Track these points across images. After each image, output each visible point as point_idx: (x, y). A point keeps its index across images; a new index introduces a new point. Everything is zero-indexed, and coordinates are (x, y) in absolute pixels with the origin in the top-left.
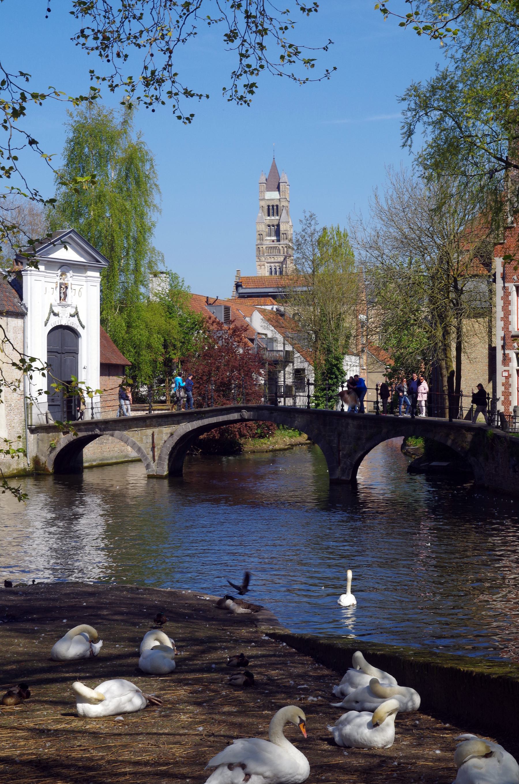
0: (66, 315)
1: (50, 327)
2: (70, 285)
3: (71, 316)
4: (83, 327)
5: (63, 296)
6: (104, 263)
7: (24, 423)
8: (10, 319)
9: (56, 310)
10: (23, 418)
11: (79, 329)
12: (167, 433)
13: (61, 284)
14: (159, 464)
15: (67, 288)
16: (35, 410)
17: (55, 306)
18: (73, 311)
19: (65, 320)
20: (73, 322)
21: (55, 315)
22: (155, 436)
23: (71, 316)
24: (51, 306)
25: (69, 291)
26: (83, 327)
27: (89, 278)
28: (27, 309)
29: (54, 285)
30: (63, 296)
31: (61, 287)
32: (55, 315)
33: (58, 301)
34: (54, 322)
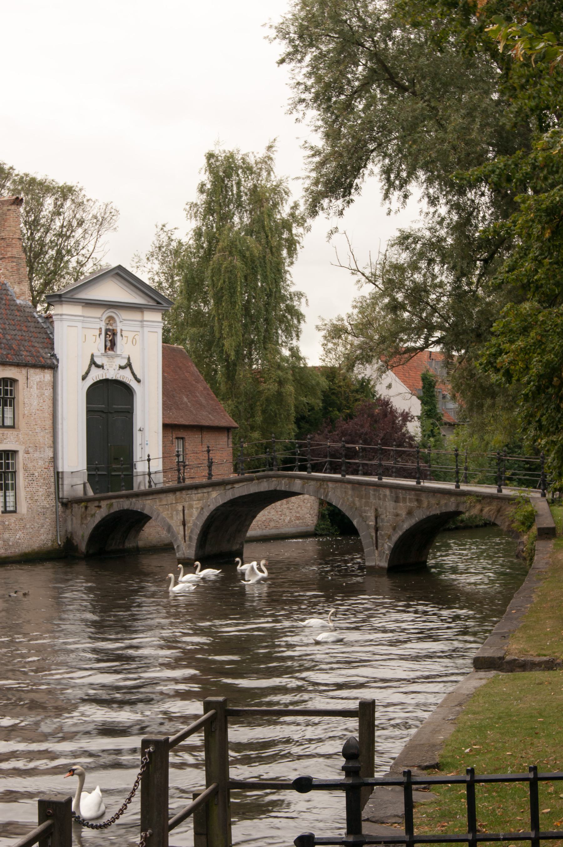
0: (114, 366)
1: (90, 381)
2: (119, 331)
3: (121, 367)
4: (139, 381)
6: (165, 305)
7: (53, 496)
8: (32, 371)
9: (98, 361)
10: (52, 489)
11: (133, 384)
12: (197, 508)
13: (107, 330)
14: (189, 546)
15: (114, 334)
16: (67, 481)
17: (98, 356)
18: (124, 362)
20: (126, 376)
22: (186, 511)
23: (121, 367)
24: (92, 356)
25: (118, 339)
26: (139, 381)
27: (145, 323)
28: (58, 360)
29: (98, 332)
30: (111, 345)
31: (106, 334)
33: (103, 351)
34: (96, 375)
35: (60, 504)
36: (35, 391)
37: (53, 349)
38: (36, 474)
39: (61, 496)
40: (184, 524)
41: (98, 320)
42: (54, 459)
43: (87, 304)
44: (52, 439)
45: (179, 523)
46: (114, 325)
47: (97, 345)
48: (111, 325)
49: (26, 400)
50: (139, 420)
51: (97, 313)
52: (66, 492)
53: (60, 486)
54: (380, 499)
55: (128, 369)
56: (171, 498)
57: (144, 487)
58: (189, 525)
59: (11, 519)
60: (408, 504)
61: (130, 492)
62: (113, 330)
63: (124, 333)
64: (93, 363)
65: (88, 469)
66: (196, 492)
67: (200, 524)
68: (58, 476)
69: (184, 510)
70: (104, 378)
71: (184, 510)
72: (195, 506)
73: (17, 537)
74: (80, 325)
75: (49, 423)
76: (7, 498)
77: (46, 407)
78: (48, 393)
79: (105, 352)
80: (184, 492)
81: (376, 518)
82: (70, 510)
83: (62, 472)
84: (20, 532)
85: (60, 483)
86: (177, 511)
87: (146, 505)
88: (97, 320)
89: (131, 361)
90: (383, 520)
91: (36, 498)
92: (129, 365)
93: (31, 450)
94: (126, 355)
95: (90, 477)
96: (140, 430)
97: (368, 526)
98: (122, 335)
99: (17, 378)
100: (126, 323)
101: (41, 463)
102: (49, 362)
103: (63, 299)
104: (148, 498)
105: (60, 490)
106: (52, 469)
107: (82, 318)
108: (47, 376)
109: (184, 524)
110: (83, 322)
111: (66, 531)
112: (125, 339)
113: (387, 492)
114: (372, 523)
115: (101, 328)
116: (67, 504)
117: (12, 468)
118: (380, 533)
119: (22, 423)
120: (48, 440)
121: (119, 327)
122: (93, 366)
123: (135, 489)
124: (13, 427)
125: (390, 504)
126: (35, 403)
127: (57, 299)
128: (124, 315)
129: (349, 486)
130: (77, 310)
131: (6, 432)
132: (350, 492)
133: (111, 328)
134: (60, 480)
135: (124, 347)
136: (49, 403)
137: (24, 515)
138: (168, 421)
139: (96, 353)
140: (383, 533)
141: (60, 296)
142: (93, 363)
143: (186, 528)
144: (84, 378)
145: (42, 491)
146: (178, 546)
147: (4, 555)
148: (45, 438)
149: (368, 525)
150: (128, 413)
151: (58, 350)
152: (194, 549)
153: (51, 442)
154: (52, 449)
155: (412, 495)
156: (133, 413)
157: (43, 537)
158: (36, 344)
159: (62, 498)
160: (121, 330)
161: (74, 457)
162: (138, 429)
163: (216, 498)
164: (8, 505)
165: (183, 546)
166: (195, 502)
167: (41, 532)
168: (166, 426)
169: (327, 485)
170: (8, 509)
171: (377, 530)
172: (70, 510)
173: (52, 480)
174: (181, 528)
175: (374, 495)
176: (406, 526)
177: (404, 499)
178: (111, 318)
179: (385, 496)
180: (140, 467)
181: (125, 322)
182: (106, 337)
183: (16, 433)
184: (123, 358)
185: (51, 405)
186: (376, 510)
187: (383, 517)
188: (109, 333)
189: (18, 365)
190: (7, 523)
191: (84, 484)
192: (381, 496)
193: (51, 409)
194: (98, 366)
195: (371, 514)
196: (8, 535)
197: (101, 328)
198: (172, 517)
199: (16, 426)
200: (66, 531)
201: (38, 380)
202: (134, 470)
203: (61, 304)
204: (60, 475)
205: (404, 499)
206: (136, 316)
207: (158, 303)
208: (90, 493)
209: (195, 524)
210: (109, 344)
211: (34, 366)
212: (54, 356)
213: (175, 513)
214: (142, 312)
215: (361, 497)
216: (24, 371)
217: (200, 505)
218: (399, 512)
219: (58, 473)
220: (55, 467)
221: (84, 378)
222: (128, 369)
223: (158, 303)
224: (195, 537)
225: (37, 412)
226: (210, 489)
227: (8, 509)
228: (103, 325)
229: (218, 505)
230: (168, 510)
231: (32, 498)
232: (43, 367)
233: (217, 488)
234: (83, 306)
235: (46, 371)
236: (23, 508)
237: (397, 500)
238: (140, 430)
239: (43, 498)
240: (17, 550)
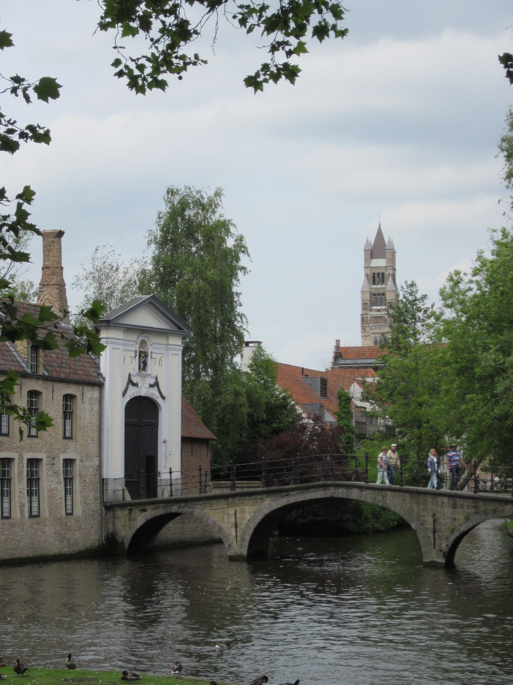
0: (146, 385)
1: (128, 398)
2: (149, 353)
3: (151, 386)
4: (163, 398)
5: (143, 366)
6: (186, 331)
7: (99, 500)
8: (86, 388)
9: (135, 380)
10: (98, 495)
11: (160, 400)
12: (250, 512)
13: (140, 352)
14: (241, 546)
15: (146, 356)
16: (111, 487)
17: (134, 376)
18: (153, 381)
19: (144, 391)
20: (153, 393)
21: (135, 385)
22: (237, 515)
23: (151, 386)
24: (130, 375)
25: (149, 360)
26: (163, 398)
27: (170, 346)
28: (104, 379)
29: (133, 354)
30: (143, 366)
31: (140, 356)
32: (135, 385)
33: (137, 371)
34: (133, 392)
35: (103, 508)
36: (87, 406)
38: (88, 480)
39: (105, 500)
41: (134, 343)
42: (100, 467)
43: (128, 328)
44: (98, 449)
46: (146, 348)
47: (133, 366)
48: (144, 348)
49: (82, 414)
51: (134, 337)
52: (110, 497)
53: (105, 491)
54: (438, 506)
55: (156, 387)
57: (166, 495)
58: (242, 526)
59: (71, 521)
60: (466, 510)
61: (153, 499)
62: (145, 352)
63: (153, 355)
64: (130, 382)
65: (126, 475)
66: (249, 498)
67: (253, 526)
68: (103, 482)
69: (236, 514)
70: (138, 395)
71: (236, 514)
72: (247, 511)
73: (76, 537)
74: (121, 347)
75: (96, 434)
76: (33, 503)
77: (94, 420)
78: (96, 407)
79: (139, 372)
80: (237, 498)
81: (434, 521)
82: (112, 513)
83: (107, 479)
84: (78, 532)
85: (105, 488)
86: (228, 515)
89: (158, 380)
90: (440, 524)
91: (88, 502)
92: (156, 384)
93: (84, 459)
94: (154, 375)
95: (128, 484)
96: (164, 442)
97: (427, 529)
98: (151, 357)
99: (76, 394)
100: (155, 347)
101: (91, 470)
103: (111, 324)
104: (197, 503)
105: (105, 495)
106: (98, 476)
107: (123, 342)
108: (94, 393)
110: (124, 345)
111: (108, 532)
112: (154, 360)
113: (446, 500)
115: (136, 351)
116: (110, 507)
117: (36, 476)
118: (438, 536)
119: (78, 435)
121: (150, 349)
122: (130, 384)
123: (159, 497)
124: (71, 438)
125: (448, 511)
126: (87, 417)
127: (105, 324)
130: (118, 334)
131: (68, 443)
132: (408, 500)
133: (143, 350)
134: (105, 485)
135: (152, 367)
136: (96, 416)
137: (80, 517)
138: (186, 435)
139: (133, 373)
140: (440, 534)
141: (108, 322)
142: (130, 382)
143: (238, 530)
144: (124, 394)
146: (230, 545)
147: (68, 553)
148: (93, 448)
149: (426, 528)
150: (154, 426)
152: (246, 548)
153: (97, 452)
154: (98, 458)
155: (470, 503)
156: (157, 427)
157: (92, 537)
158: (85, 364)
159: (106, 502)
160: (151, 353)
161: (115, 467)
162: (163, 441)
164: (33, 510)
165: (235, 545)
166: (247, 507)
167: (91, 532)
168: (185, 440)
169: (386, 494)
170: (33, 514)
171: (434, 532)
172: (112, 513)
173: (99, 486)
174: (233, 530)
175: (433, 502)
177: (462, 506)
178: (143, 343)
179: (443, 503)
180: (164, 476)
181: (154, 345)
182: (139, 359)
183: (75, 443)
184: (152, 377)
185: (98, 419)
186: (434, 515)
187: (441, 520)
188: (143, 355)
190: (69, 524)
191: (123, 490)
192: (440, 503)
193: (98, 422)
195: (430, 520)
196: (69, 535)
197: (136, 351)
198: (223, 520)
199: (73, 437)
200: (108, 532)
201: (90, 396)
202: (159, 478)
203: (107, 329)
204: (105, 481)
205: (462, 506)
206: (162, 340)
207: (180, 328)
208: (128, 498)
209: (247, 527)
210: (142, 365)
212: (100, 374)
213: (226, 516)
214: (167, 337)
215: (419, 504)
216: (81, 388)
217: (253, 510)
218: (457, 517)
219: (103, 479)
220: (100, 474)
221: (124, 394)
222: (156, 387)
223: (180, 328)
225: (89, 425)
226: (264, 496)
227: (33, 514)
228: (137, 348)
229: (272, 509)
230: (219, 513)
231: (85, 502)
233: (271, 495)
234: (124, 331)
235: (95, 388)
237: (455, 507)
238: (164, 442)
239: (92, 502)
240: (76, 549)
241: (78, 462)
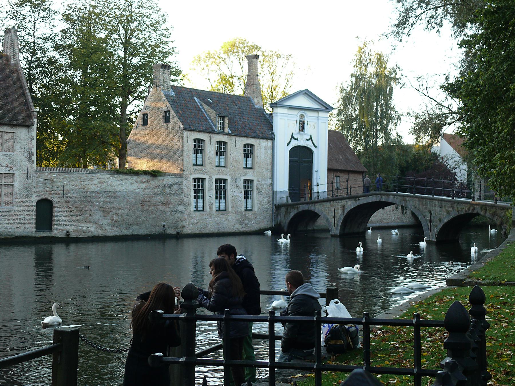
4: (316, 147)
11: (313, 148)
13: (300, 121)
15: (303, 123)
18: (308, 138)
20: (309, 144)
26: (316, 147)
36: (263, 150)
37: (272, 130)
40: (334, 218)
42: (272, 185)
45: (332, 217)
50: (315, 167)
51: (295, 112)
52: (278, 201)
56: (328, 204)
64: (292, 137)
67: (342, 217)
68: (274, 193)
74: (286, 118)
75: (270, 167)
78: (270, 152)
87: (317, 208)
88: (296, 115)
92: (311, 138)
93: (260, 180)
100: (310, 118)
101: (265, 186)
102: (270, 136)
108: (269, 143)
109: (334, 218)
113: (437, 202)
114: (428, 219)
116: (278, 207)
120: (269, 175)
124: (251, 168)
125: (438, 209)
128: (309, 114)
129: (417, 199)
144: (288, 145)
145: (266, 200)
150: (310, 163)
151: (275, 131)
161: (282, 183)
163: (350, 205)
171: (431, 221)
176: (446, 221)
178: (302, 116)
179: (435, 205)
189: (254, 138)
194: (295, 139)
206: (315, 114)
211: (263, 138)
212: (273, 133)
216: (257, 140)
220: (272, 188)
221: (288, 145)
224: (340, 224)
232: (267, 139)
236: (256, 209)
237: (441, 207)
241: (255, 182)
